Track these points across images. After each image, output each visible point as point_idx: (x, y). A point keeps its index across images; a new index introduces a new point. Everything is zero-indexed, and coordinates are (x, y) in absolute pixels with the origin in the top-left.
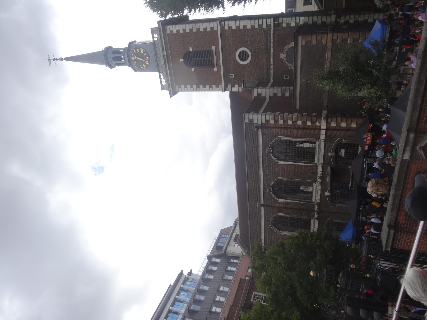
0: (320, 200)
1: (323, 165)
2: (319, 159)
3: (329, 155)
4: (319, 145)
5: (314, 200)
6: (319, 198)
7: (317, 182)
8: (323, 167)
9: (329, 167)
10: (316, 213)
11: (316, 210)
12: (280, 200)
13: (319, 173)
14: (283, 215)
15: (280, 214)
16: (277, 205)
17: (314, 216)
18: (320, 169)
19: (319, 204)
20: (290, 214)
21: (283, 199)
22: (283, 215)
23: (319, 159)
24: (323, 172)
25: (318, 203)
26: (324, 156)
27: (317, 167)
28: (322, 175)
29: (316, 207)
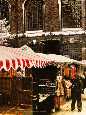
0: (28, 37)
1: (61, 36)
2: (65, 31)
3: (71, 39)
4: (79, 30)
5: (27, 32)
6: (30, 36)
7: (44, 32)
8: (59, 35)
9: (59, 40)
10: (16, 35)
11: (19, 35)
12: (23, 5)
13: (54, 33)
14: (10, 10)
15: (10, 7)
16: (19, 4)
17: (12, 34)
18: (57, 33)
19: (24, 37)
20: (12, 15)
21: (25, 8)
22: (10, 10)
23: (65, 31)
24: (55, 36)
25: (25, 35)
26: (69, 35)
27: (59, 31)
28: (52, 36)
29: (21, 35)
